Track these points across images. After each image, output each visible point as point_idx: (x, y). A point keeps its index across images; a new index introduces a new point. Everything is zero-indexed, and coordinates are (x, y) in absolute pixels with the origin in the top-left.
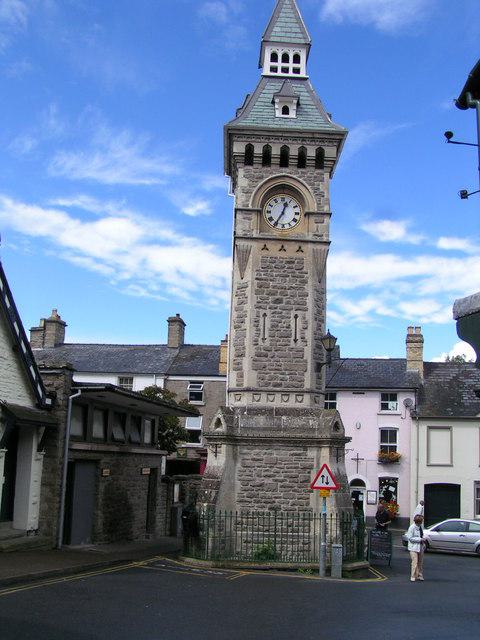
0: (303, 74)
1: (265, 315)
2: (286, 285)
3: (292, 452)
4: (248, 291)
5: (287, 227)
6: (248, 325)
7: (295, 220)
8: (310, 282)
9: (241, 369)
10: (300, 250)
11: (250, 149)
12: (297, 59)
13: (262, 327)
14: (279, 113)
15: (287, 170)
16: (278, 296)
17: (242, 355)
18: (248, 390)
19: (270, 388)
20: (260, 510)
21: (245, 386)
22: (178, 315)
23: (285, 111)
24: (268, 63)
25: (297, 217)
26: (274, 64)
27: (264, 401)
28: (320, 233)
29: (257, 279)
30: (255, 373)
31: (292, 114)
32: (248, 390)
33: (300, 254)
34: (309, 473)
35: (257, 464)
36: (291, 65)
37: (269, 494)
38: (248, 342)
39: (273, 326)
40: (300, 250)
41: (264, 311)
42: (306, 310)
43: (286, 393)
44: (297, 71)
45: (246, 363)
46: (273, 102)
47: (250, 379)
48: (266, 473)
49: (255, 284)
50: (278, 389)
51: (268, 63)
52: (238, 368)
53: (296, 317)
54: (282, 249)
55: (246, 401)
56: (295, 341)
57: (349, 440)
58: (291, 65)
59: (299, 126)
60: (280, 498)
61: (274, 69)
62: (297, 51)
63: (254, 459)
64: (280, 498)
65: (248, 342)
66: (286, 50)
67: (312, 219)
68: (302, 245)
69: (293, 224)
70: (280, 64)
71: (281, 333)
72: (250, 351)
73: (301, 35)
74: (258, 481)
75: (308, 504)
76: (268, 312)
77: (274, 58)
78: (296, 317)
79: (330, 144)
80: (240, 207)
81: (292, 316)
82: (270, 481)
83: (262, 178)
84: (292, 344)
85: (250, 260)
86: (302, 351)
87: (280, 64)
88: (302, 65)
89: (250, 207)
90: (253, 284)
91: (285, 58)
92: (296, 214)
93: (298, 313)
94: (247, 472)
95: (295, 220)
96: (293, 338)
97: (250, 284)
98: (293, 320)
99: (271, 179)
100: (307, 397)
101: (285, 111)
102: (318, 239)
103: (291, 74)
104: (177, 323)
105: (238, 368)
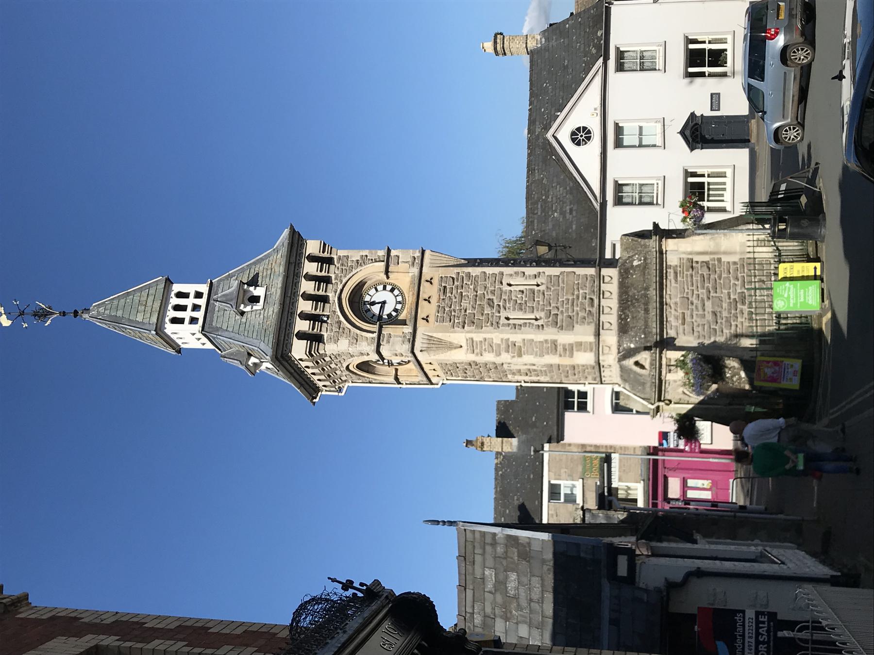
0: (204, 288)
1: (508, 319)
2: (471, 294)
3: (673, 281)
5: (399, 299)
6: (517, 337)
7: (392, 290)
9: (571, 345)
12: (180, 295)
13: (522, 321)
16: (485, 302)
17: (554, 343)
18: (598, 334)
19: (594, 310)
20: (746, 315)
21: (591, 339)
25: (389, 288)
26: (187, 321)
27: (611, 318)
28: (410, 260)
29: (463, 327)
30: (577, 327)
31: (259, 292)
32: (598, 334)
33: (436, 281)
34: (697, 262)
35: (688, 319)
36: (189, 302)
37: (725, 305)
38: (539, 337)
41: (503, 318)
43: (600, 294)
44: (199, 295)
45: (565, 338)
47: (584, 334)
48: (700, 308)
50: (596, 302)
52: (570, 350)
53: (510, 285)
55: (610, 338)
57: (656, 225)
59: (278, 283)
60: (729, 294)
63: (683, 324)
64: (729, 294)
65: (539, 337)
68: (423, 280)
69: (396, 292)
70: (186, 315)
72: (550, 334)
73: (152, 291)
74: (709, 317)
75: (735, 263)
76: (503, 314)
78: (510, 285)
82: (708, 304)
84: (542, 288)
86: (550, 276)
89: (375, 335)
91: (177, 308)
92: (385, 288)
94: (700, 329)
95: (392, 290)
96: (535, 287)
97: (469, 335)
101: (255, 299)
102: (418, 261)
103: (202, 302)
105: (570, 350)
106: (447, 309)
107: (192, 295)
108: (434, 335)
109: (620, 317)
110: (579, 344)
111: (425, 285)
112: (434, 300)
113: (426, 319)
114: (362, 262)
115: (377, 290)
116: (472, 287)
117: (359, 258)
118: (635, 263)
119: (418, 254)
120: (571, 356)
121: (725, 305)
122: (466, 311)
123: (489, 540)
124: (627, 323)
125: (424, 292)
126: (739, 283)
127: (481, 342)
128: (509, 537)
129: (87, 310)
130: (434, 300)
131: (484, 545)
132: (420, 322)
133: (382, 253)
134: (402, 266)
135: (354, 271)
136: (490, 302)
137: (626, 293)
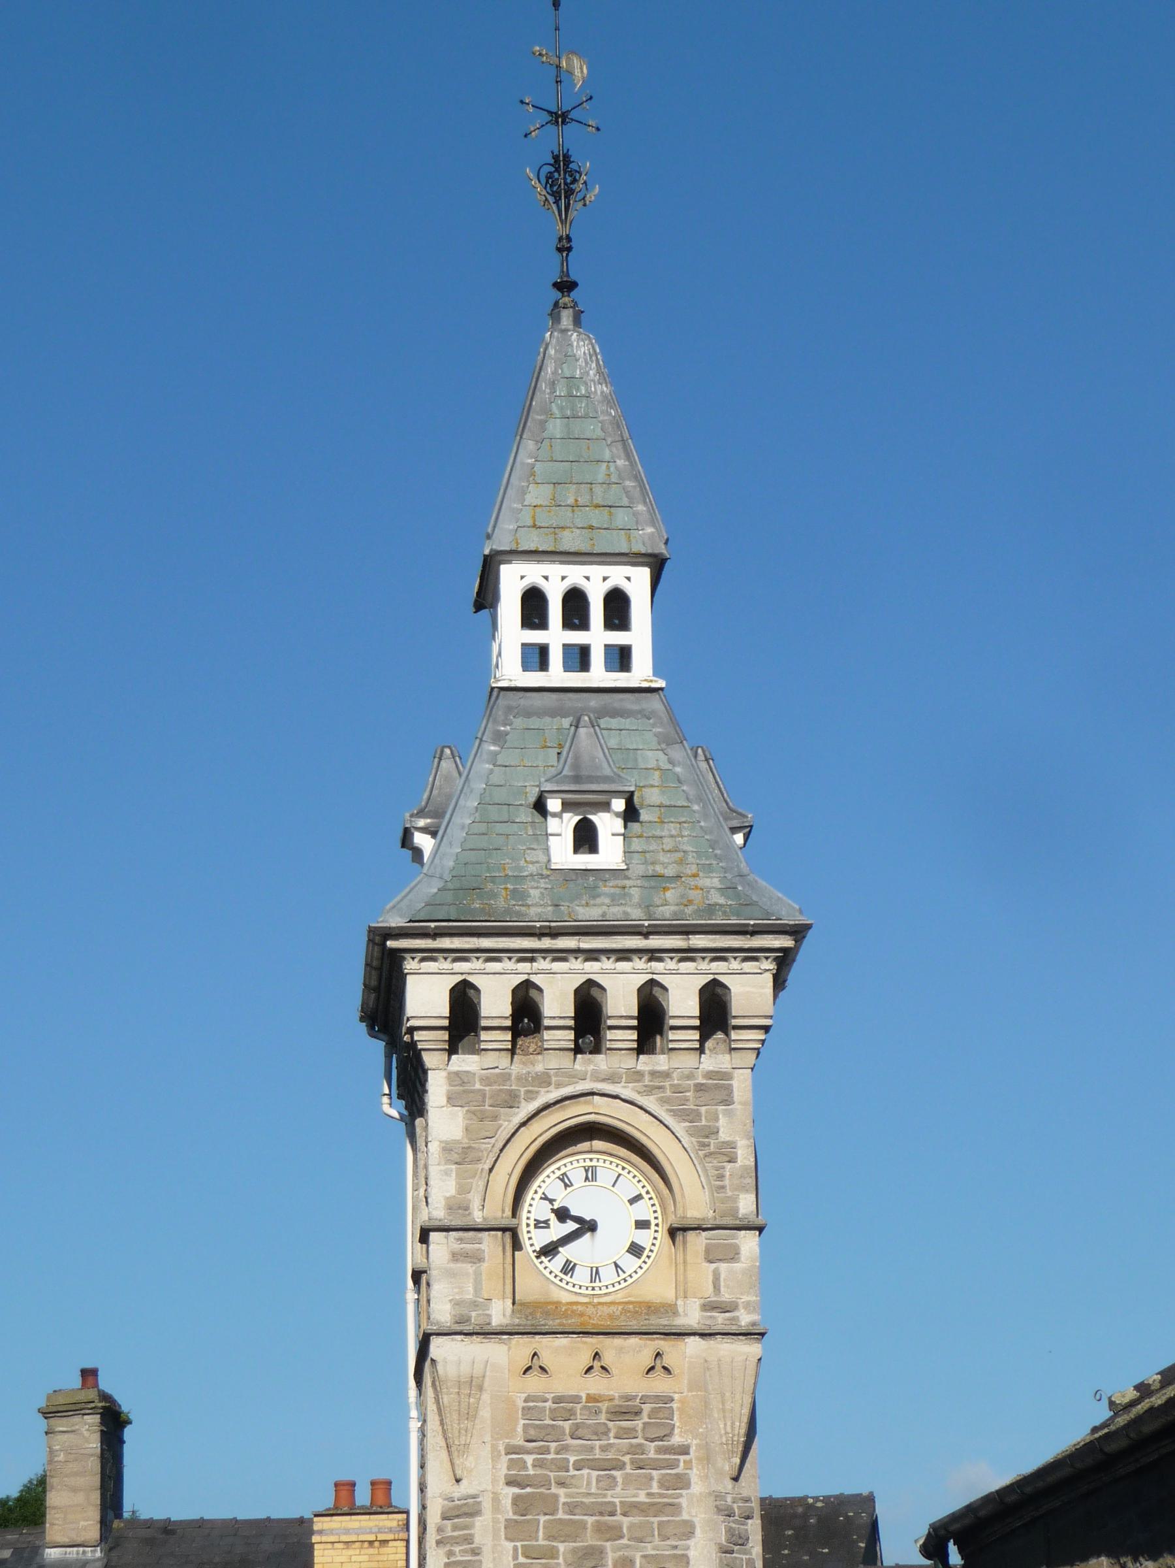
0: (642, 672)
2: (616, 1496)
4: (483, 1529)
7: (635, 1250)
8: (697, 1487)
10: (657, 1366)
11: (464, 1001)
12: (617, 608)
14: (561, 850)
15: (601, 1062)
16: (590, 1539)
22: (89, 1375)
23: (586, 838)
24: (511, 632)
25: (644, 1238)
26: (535, 637)
28: (726, 1296)
29: (509, 1483)
31: (610, 851)
33: (659, 1385)
36: (597, 637)
40: (657, 1366)
44: (621, 658)
46: (540, 806)
49: (507, 1503)
54: (596, 1365)
58: (597, 637)
61: (538, 657)
66: (575, 574)
67: (697, 1242)
69: (631, 1263)
70: (556, 636)
77: (533, 607)
79: (749, 966)
80: (438, 1212)
83: (511, 1102)
85: (485, 1413)
87: (556, 636)
88: (639, 636)
90: (496, 1499)
91: (575, 603)
92: (642, 1225)
95: (635, 1250)
97: (486, 1504)
99: (547, 1107)
101: (586, 838)
102: (720, 1320)
103: (599, 675)
106: (567, 1425)
107: (618, 638)
108: (486, 1397)
111: (640, 1351)
112: (596, 1384)
114: (712, 1150)
115: (632, 1201)
116: (642, 1497)
117: (724, 1136)
119: (745, 1319)
122: (561, 1484)
125: (620, 1350)
127: (469, 1539)
129: (577, 321)
130: (596, 1384)
132: (522, 1347)
133: (746, 1205)
134: (702, 1274)
135: (679, 1128)
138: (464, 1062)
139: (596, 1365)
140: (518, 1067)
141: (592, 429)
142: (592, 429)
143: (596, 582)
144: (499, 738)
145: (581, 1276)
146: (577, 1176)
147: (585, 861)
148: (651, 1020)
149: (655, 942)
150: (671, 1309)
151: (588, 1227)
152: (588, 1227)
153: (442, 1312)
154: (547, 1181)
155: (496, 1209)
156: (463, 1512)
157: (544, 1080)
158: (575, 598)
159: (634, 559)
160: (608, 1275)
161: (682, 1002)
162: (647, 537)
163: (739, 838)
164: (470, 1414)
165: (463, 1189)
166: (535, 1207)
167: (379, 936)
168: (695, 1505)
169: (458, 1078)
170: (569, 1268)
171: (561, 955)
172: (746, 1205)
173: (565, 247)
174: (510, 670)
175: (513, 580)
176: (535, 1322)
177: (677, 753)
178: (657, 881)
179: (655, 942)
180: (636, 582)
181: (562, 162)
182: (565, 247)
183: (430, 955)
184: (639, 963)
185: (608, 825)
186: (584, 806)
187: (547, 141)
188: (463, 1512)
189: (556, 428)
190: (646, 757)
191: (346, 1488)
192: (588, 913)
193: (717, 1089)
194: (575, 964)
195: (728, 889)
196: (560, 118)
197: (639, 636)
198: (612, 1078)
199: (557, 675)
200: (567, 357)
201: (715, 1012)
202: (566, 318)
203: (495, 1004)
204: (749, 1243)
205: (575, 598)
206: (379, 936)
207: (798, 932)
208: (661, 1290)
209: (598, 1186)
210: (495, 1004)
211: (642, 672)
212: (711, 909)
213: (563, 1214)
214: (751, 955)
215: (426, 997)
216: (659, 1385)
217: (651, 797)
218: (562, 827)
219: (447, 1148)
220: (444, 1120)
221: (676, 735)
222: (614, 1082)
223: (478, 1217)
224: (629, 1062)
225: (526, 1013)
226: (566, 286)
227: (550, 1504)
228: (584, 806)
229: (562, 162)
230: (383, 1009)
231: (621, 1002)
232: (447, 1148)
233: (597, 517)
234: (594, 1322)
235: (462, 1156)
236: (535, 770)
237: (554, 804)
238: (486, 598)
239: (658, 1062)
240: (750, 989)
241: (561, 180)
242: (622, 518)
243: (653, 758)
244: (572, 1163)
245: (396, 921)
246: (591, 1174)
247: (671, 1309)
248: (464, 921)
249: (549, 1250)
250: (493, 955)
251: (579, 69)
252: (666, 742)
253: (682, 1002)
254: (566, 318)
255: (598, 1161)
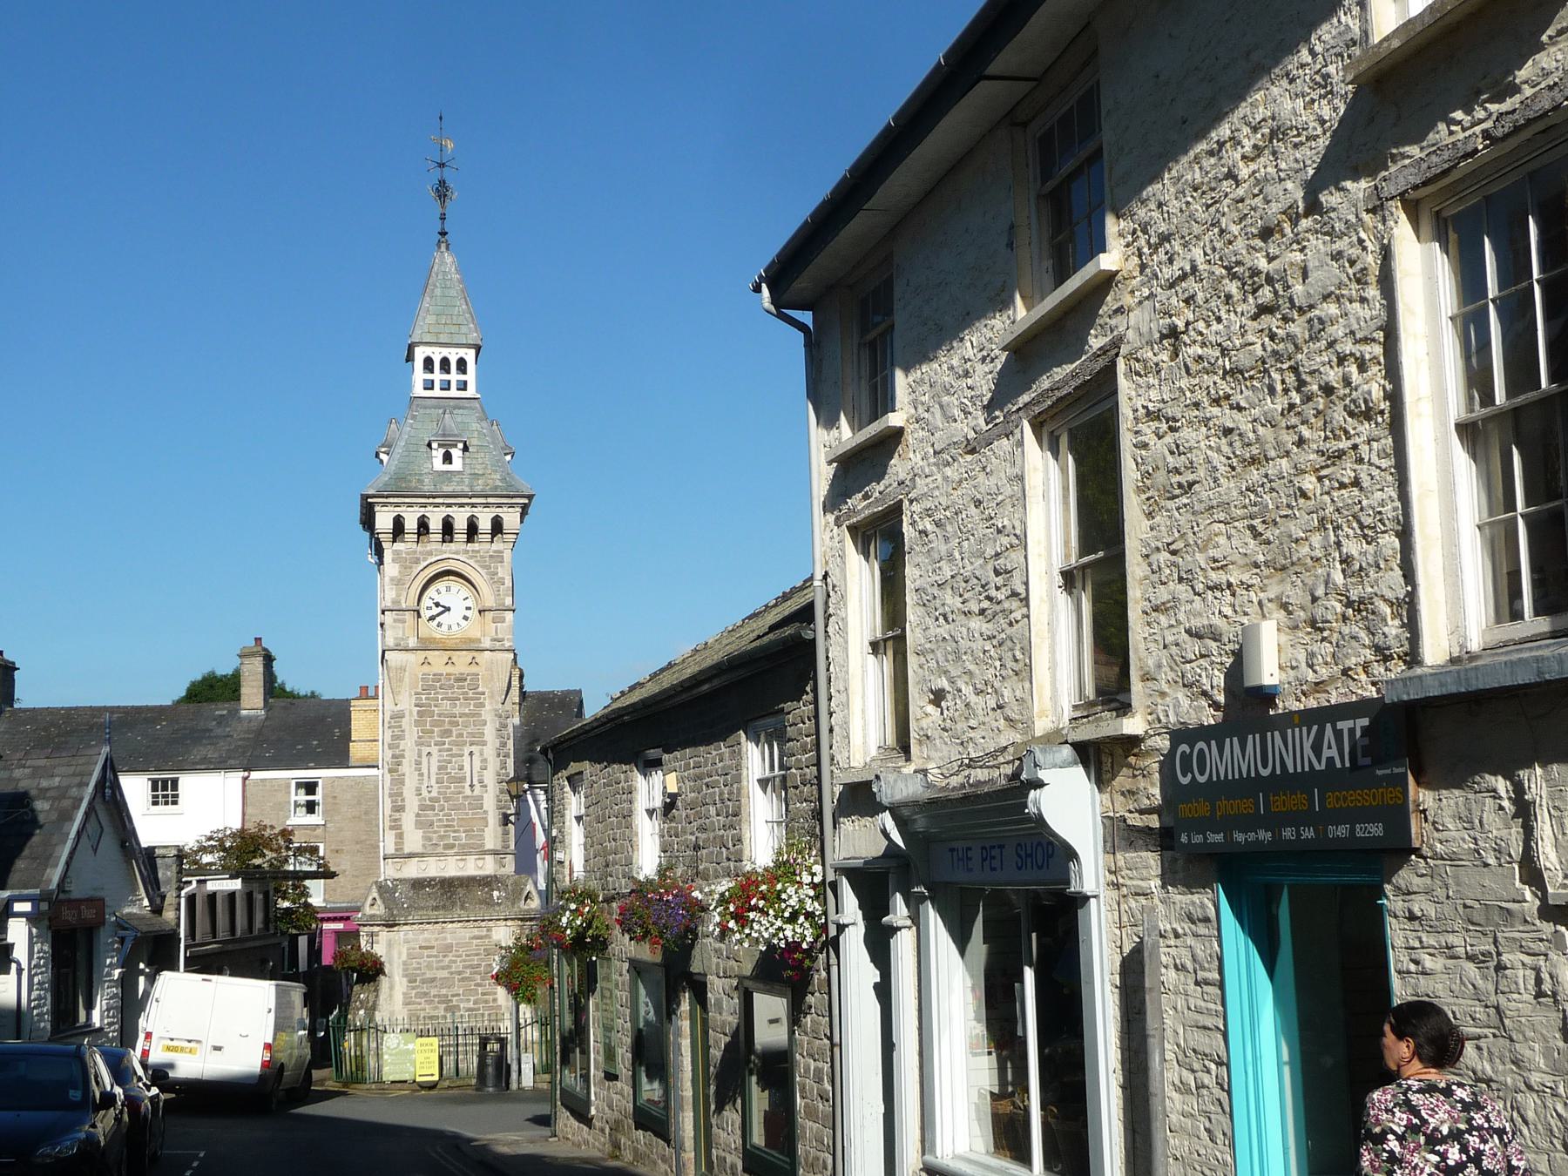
0: (471, 392)
2: (456, 711)
4: (405, 722)
7: (466, 618)
8: (488, 707)
9: (399, 827)
12: (462, 364)
13: (425, 771)
14: (438, 464)
19: (440, 849)
22: (258, 640)
23: (448, 458)
24: (419, 375)
25: (468, 613)
26: (429, 376)
31: (457, 465)
33: (474, 669)
35: (426, 952)
36: (454, 376)
39: (440, 768)
40: (473, 662)
41: (428, 749)
42: (484, 743)
44: (463, 386)
46: (429, 445)
47: (414, 841)
51: (419, 375)
53: (471, 754)
54: (450, 661)
56: (471, 786)
58: (454, 376)
61: (429, 385)
62: (462, 352)
65: (408, 792)
66: (445, 352)
67: (490, 615)
69: (463, 623)
70: (437, 376)
71: (451, 778)
72: (412, 804)
74: (429, 975)
75: (495, 1000)
76: (434, 750)
77: (428, 364)
78: (471, 754)
80: (389, 604)
81: (466, 753)
82: (444, 974)
83: (417, 561)
84: (468, 792)
85: (407, 680)
88: (471, 376)
91: (445, 364)
93: (473, 748)
95: (466, 618)
98: (467, 758)
100: (489, 858)
101: (448, 458)
103: (454, 393)
104: (258, 640)
105: (396, 826)
107: (462, 377)
109: (433, 879)
110: (400, 836)
111: (467, 656)
112: (449, 669)
113: (425, 662)
114: (495, 580)
118: (496, 894)
119: (507, 644)
120: (391, 828)
121: (444, 991)
123: (85, 779)
124: (424, 887)
126: (471, 1005)
128: (81, 800)
130: (449, 669)
131: (81, 774)
132: (421, 655)
135: (483, 572)
136: (447, 733)
137: (461, 885)
138: (399, 546)
139: (450, 661)
140: (420, 548)
141: (453, 293)
142: (453, 293)
143: (453, 355)
144: (414, 417)
145: (444, 628)
146: (443, 590)
147: (447, 467)
148: (472, 530)
149: (474, 500)
150: (479, 641)
151: (448, 609)
152: (448, 609)
153: (390, 642)
154: (431, 591)
155: (412, 603)
156: (398, 716)
157: (430, 553)
158: (444, 358)
159: (468, 346)
160: (455, 628)
161: (485, 524)
162: (474, 337)
163: (508, 458)
164: (401, 680)
165: (398, 595)
166: (426, 602)
167: (365, 497)
168: (487, 713)
169: (396, 552)
170: (439, 625)
171: (437, 505)
172: (508, 601)
173: (443, 218)
174: (419, 390)
175: (420, 353)
176: (426, 645)
177: (484, 424)
178: (475, 476)
179: (474, 500)
180: (469, 355)
181: (442, 183)
182: (443, 218)
183: (385, 505)
184: (468, 508)
185: (456, 453)
186: (447, 446)
187: (436, 174)
188: (398, 716)
189: (438, 292)
190: (474, 429)
191: (364, 689)
192: (447, 489)
193: (498, 558)
194: (443, 508)
195: (503, 480)
196: (442, 165)
197: (471, 376)
198: (457, 553)
199: (437, 392)
200: (443, 263)
201: (497, 527)
202: (443, 246)
203: (411, 524)
204: (509, 616)
205: (444, 358)
206: (365, 497)
207: (530, 497)
208: (476, 634)
209: (451, 594)
210: (411, 524)
211: (471, 392)
212: (496, 487)
213: (437, 605)
214: (512, 505)
215: (384, 521)
216: (474, 669)
217: (473, 442)
218: (438, 454)
219: (392, 579)
220: (391, 568)
221: (484, 417)
222: (456, 553)
223: (404, 606)
224: (464, 546)
225: (423, 526)
226: (443, 234)
227: (432, 714)
228: (447, 446)
229: (442, 183)
230: (368, 521)
231: (460, 524)
232: (392, 579)
233: (454, 329)
234: (450, 646)
235: (397, 582)
236: (427, 431)
237: (435, 445)
238: (410, 358)
239: (476, 546)
240: (511, 518)
241: (442, 191)
242: (464, 329)
243: (475, 426)
244: (440, 585)
245: (371, 492)
246: (448, 589)
247: (479, 641)
248: (400, 491)
249: (432, 618)
250: (410, 505)
251: (450, 145)
252: (480, 419)
253: (485, 524)
254: (443, 246)
255: (452, 584)
